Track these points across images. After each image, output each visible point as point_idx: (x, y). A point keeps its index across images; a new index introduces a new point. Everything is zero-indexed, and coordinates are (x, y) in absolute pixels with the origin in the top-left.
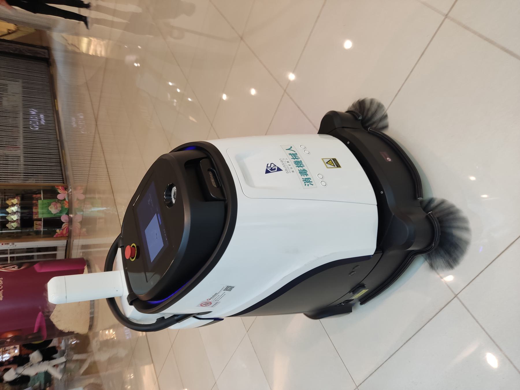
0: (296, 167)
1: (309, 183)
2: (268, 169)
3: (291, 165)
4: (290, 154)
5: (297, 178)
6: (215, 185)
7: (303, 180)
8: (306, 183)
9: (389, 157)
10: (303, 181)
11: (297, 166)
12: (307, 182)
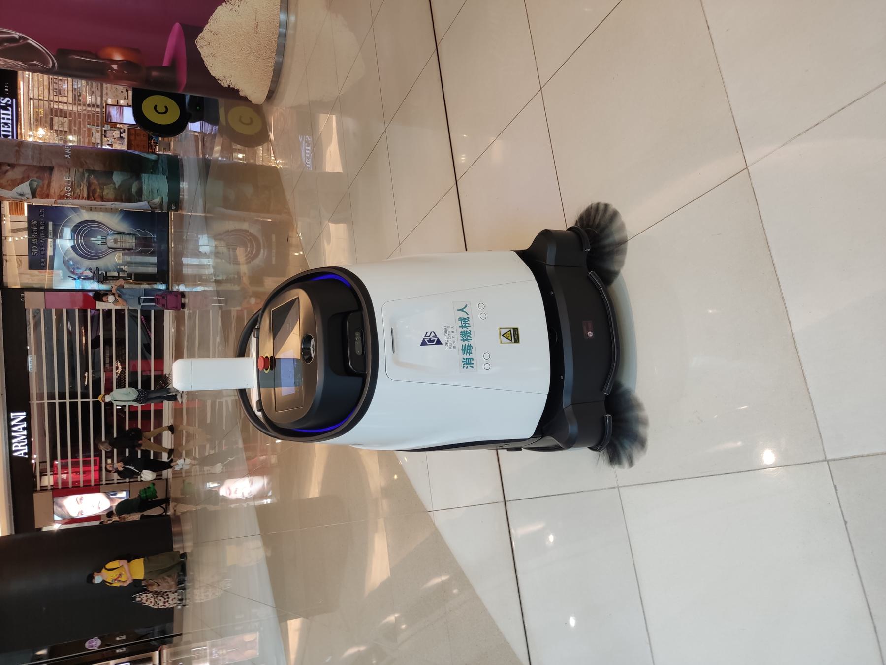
0: (461, 340)
1: (468, 365)
2: (426, 340)
3: (456, 337)
4: (460, 319)
5: (458, 355)
6: (359, 352)
7: (464, 360)
8: (465, 365)
9: (591, 331)
10: (463, 361)
11: (462, 339)
12: (467, 364)
